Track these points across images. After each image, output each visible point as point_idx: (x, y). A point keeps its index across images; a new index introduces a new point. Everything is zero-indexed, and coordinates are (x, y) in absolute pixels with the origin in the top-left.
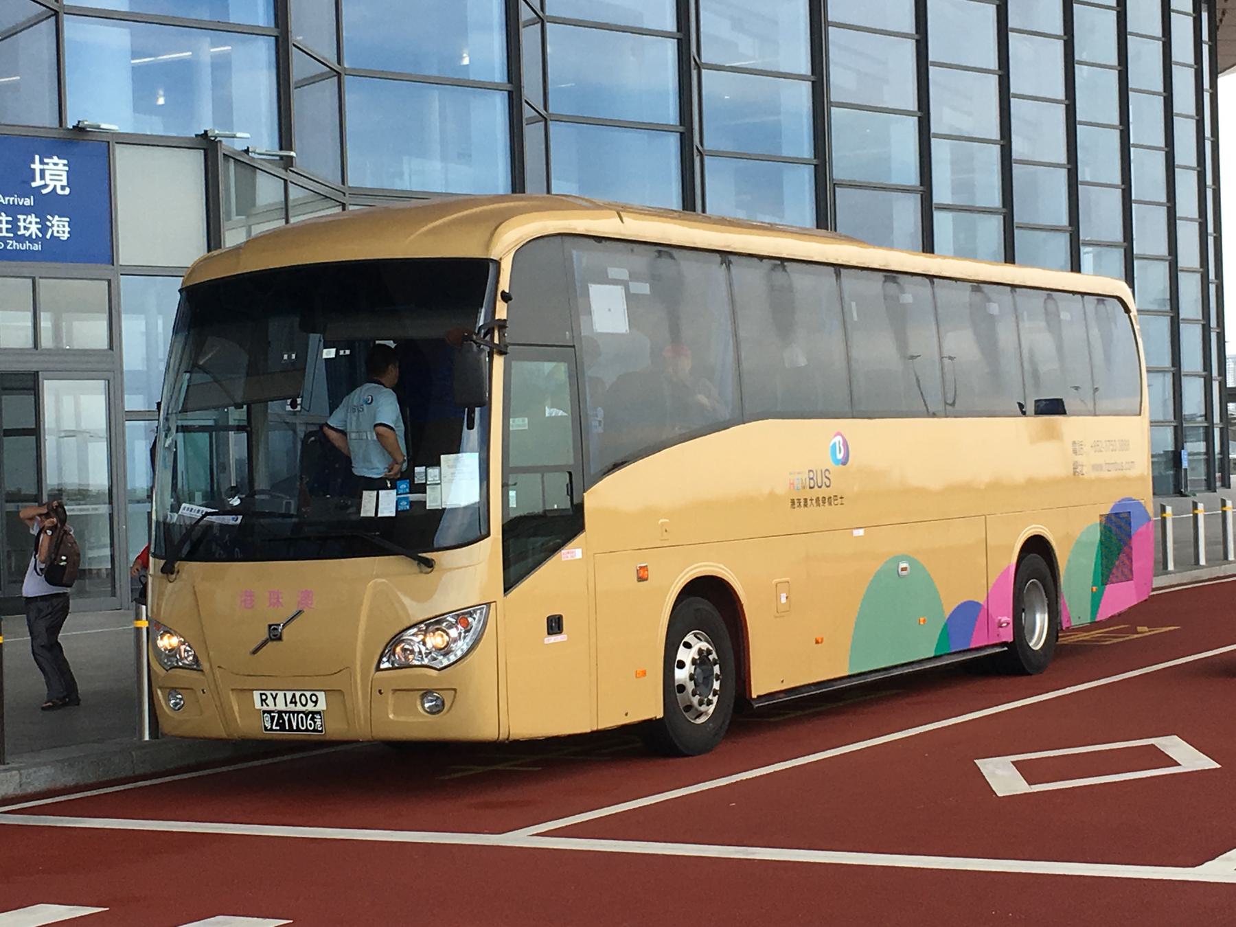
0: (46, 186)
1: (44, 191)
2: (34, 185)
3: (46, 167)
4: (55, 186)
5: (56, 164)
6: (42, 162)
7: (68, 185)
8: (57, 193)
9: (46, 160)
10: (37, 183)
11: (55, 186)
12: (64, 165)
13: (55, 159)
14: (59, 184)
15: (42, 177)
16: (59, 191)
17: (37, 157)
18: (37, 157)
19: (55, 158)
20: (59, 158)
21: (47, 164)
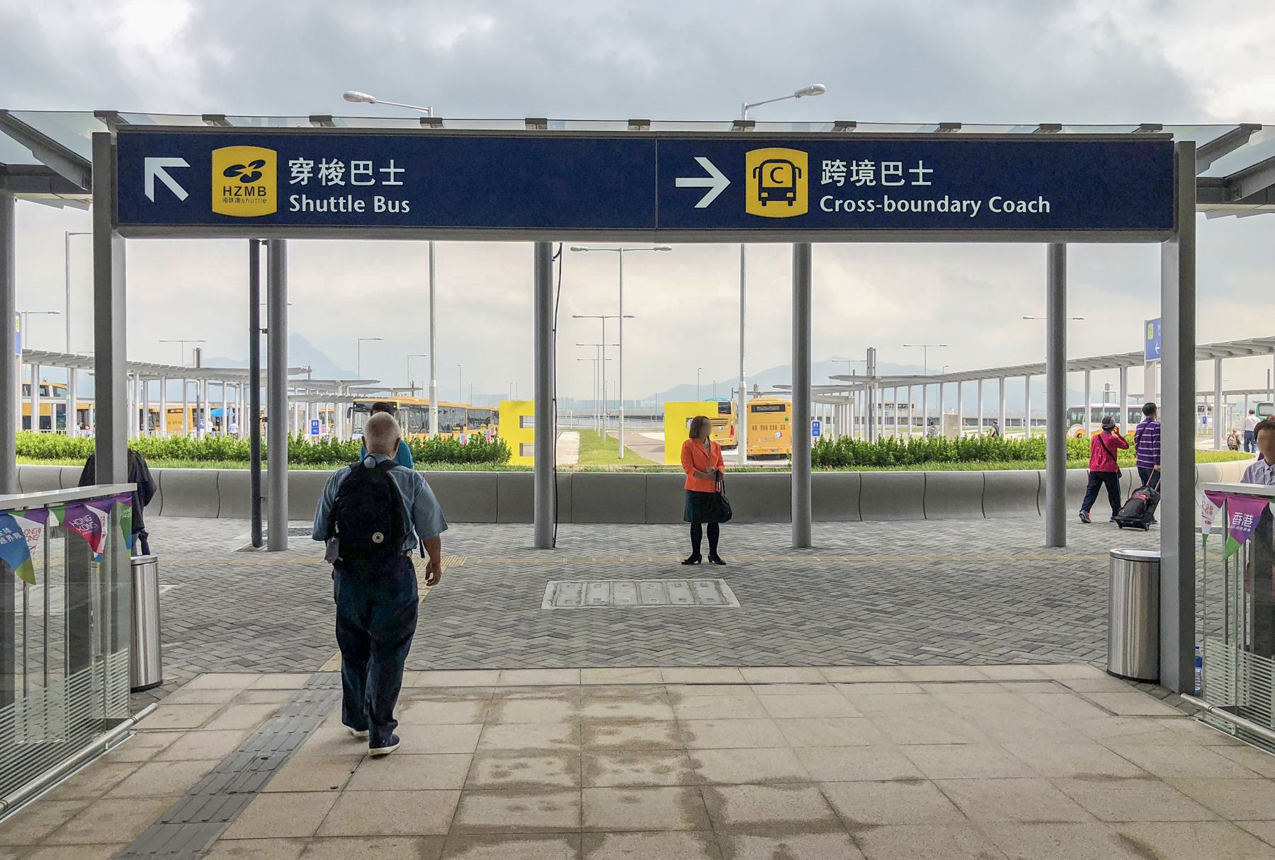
0: (859, 181)
1: (858, 184)
2: (852, 179)
3: (860, 168)
4: (866, 180)
5: (866, 165)
6: (858, 165)
7: (875, 179)
8: (1049, 202)
9: (860, 163)
10: (854, 178)
11: (866, 180)
12: (872, 166)
13: (867, 162)
14: (868, 179)
15: (857, 174)
16: (869, 184)
17: (854, 162)
18: (854, 162)
19: (866, 161)
20: (869, 161)
21: (861, 165)
